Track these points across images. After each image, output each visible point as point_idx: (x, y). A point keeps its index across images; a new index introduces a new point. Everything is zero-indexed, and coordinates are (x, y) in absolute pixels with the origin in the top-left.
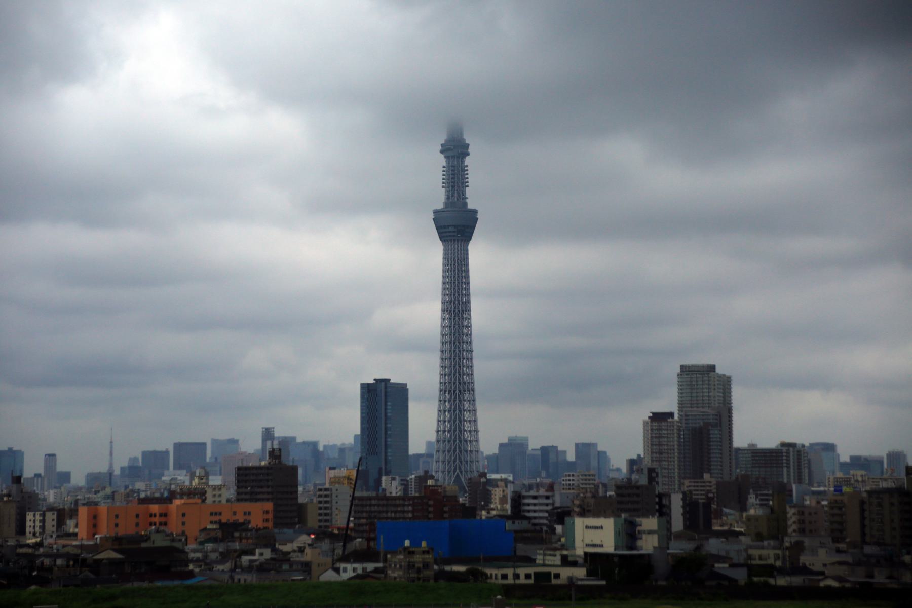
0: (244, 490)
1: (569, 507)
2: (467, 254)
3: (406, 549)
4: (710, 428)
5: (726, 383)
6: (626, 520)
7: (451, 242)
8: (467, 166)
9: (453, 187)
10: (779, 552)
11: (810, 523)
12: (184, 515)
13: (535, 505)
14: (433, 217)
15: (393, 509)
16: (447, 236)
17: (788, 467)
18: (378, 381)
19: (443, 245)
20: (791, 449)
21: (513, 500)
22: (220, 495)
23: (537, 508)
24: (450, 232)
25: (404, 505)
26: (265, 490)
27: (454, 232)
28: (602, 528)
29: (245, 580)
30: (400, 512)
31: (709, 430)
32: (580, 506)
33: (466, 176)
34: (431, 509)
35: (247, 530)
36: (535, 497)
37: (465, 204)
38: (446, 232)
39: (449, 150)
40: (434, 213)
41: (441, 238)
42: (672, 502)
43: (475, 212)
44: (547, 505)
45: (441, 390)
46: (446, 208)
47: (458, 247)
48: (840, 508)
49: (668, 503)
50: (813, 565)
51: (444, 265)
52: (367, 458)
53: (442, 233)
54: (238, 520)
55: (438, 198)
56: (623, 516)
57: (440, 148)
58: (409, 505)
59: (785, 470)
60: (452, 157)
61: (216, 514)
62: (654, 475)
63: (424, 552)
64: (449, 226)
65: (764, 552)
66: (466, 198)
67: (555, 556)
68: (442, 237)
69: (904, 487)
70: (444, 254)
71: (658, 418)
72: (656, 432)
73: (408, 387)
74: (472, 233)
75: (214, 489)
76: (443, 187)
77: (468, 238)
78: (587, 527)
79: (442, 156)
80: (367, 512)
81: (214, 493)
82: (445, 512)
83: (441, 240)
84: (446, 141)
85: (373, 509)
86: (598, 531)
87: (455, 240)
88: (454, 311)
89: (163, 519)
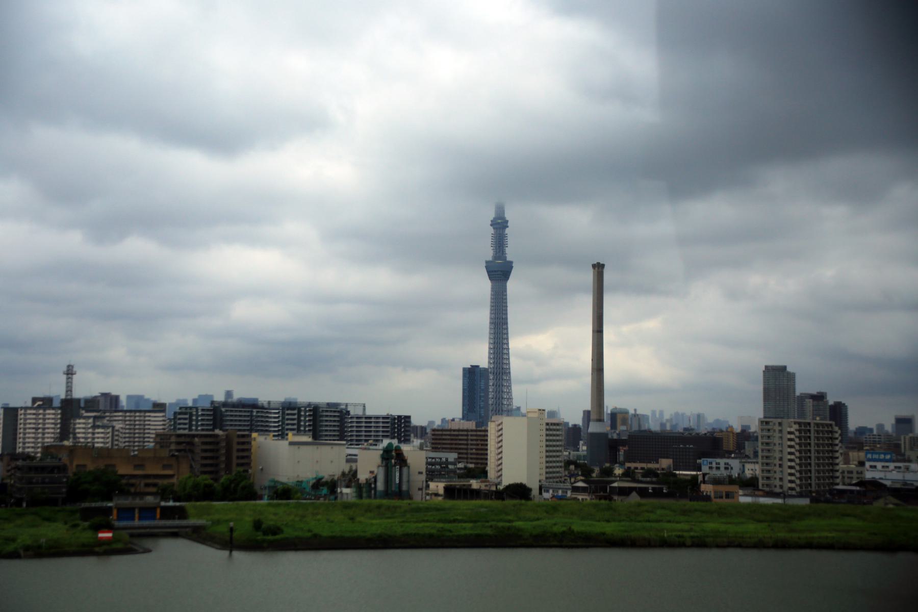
8: (507, 234)
9: (499, 247)
19: (491, 283)
24: (498, 275)
27: (500, 275)
37: (506, 257)
43: (511, 262)
52: (467, 414)
55: (488, 253)
57: (490, 223)
60: (500, 228)
64: (498, 271)
68: (490, 278)
74: (509, 276)
79: (492, 228)
84: (494, 218)
88: (500, 324)
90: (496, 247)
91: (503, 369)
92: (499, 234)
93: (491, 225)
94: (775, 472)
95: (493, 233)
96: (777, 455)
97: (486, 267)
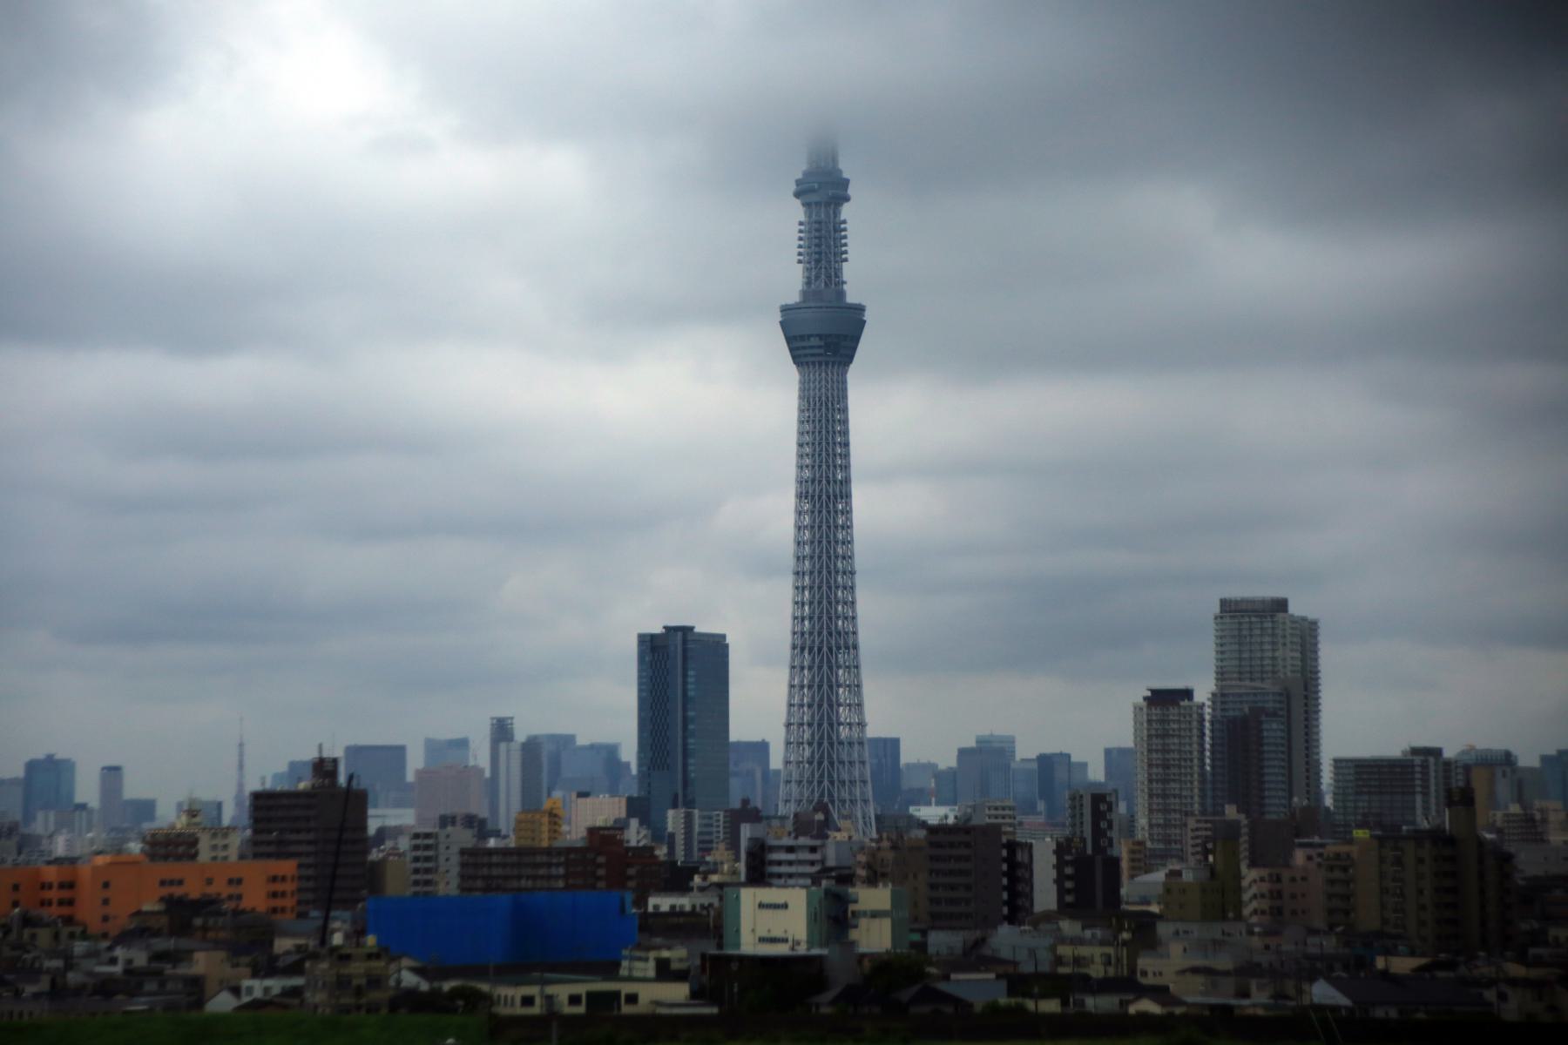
0: (264, 837)
1: (849, 868)
2: (845, 390)
3: (334, 949)
4: (1263, 718)
5: (1307, 634)
6: (827, 892)
7: (814, 367)
8: (844, 222)
9: (818, 261)
10: (1110, 950)
11: (1293, 896)
12: (106, 885)
13: (790, 863)
15: (529, 871)
16: (806, 355)
17: (1426, 794)
19: (800, 373)
20: (1432, 760)
21: (750, 854)
22: (225, 847)
23: (792, 869)
24: (812, 347)
25: (550, 865)
26: (302, 836)
27: (820, 347)
28: (785, 906)
29: (31, 1014)
30: (542, 877)
31: (1261, 723)
32: (869, 866)
33: (843, 241)
34: (601, 872)
35: (219, 914)
36: (790, 849)
37: (841, 294)
38: (804, 348)
39: (812, 191)
40: (781, 311)
42: (1035, 858)
43: (860, 309)
44: (812, 863)
45: (794, 647)
46: (804, 302)
47: (827, 375)
48: (1345, 869)
49: (1026, 860)
50: (1161, 974)
51: (801, 411)
53: (798, 348)
54: (187, 895)
55: (790, 282)
56: (824, 883)
57: (793, 187)
58: (558, 865)
59: (1419, 798)
60: (817, 204)
61: (172, 883)
62: (1103, 807)
63: (370, 956)
64: (809, 336)
65: (1084, 951)
66: (844, 283)
67: (646, 960)
68: (798, 357)
69: (1444, 831)
70: (800, 389)
71: (1164, 700)
72: (1158, 726)
73: (728, 640)
74: (854, 349)
75: (214, 835)
76: (800, 262)
77: (849, 358)
78: (761, 906)
79: (798, 203)
80: (484, 878)
81: (214, 842)
82: (630, 878)
83: (795, 363)
84: (806, 174)
85: (496, 872)
86: (781, 912)
88: (820, 497)
89: (65, 894)
97: (781, 323)
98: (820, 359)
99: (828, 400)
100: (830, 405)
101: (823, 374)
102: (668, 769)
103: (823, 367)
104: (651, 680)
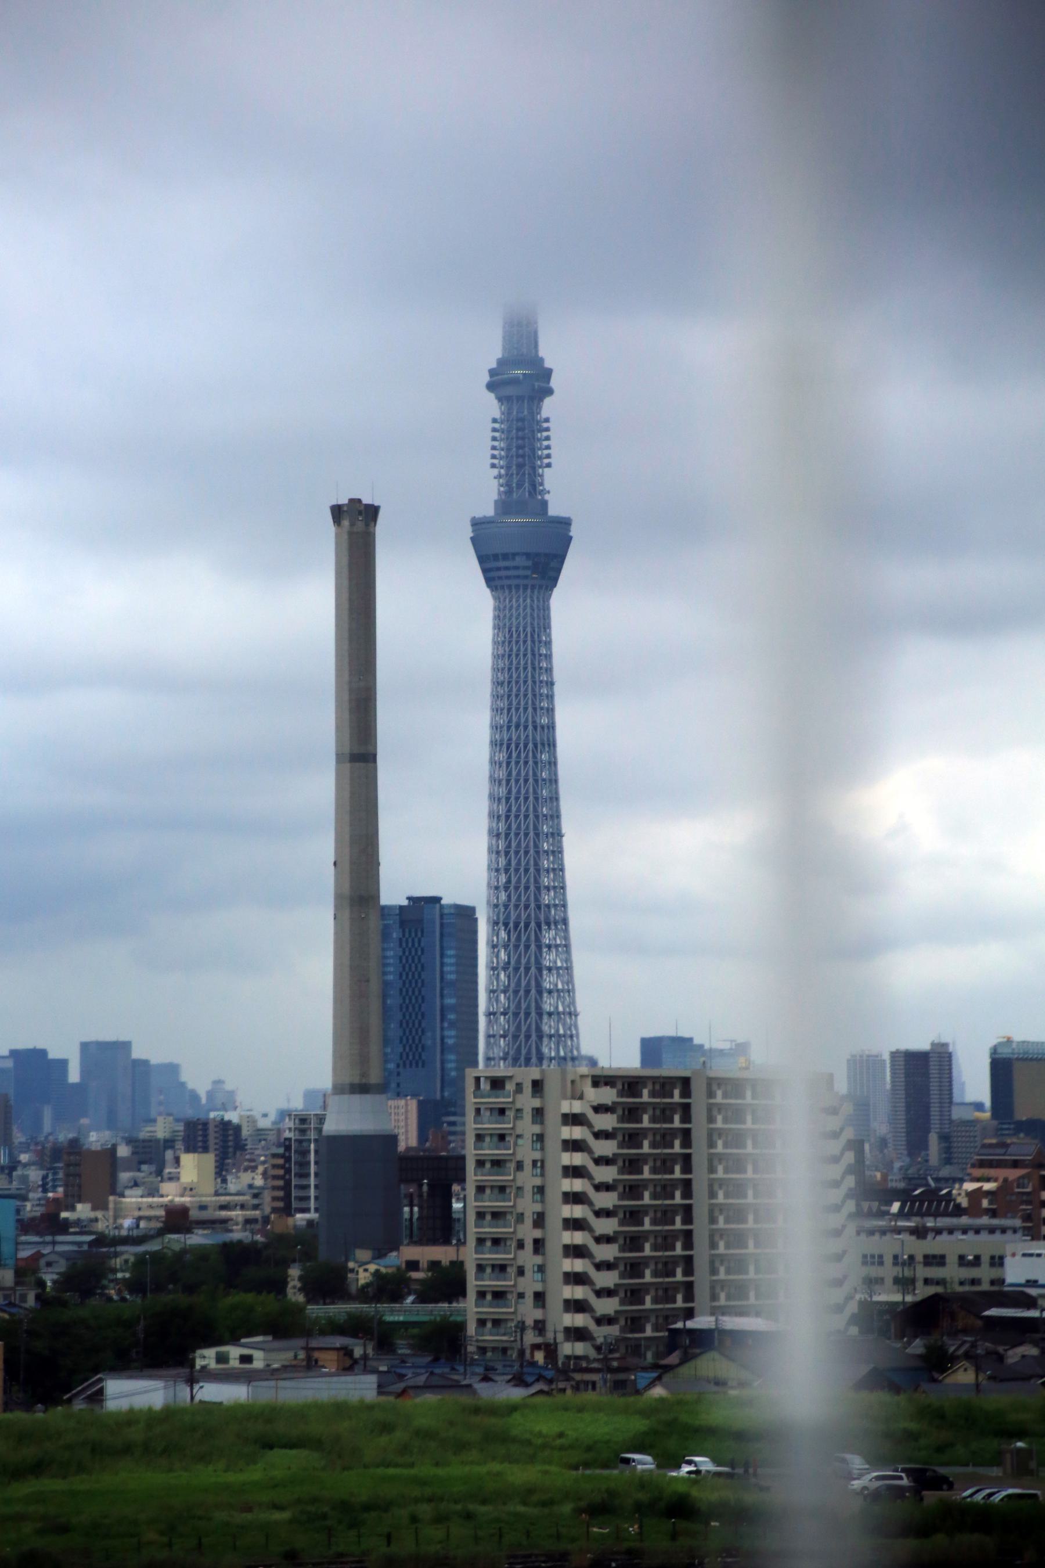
7: (510, 592)
9: (520, 466)
14: (472, 535)
16: (508, 577)
18: (416, 902)
24: (516, 568)
27: (526, 568)
37: (545, 504)
40: (472, 525)
41: (490, 581)
43: (565, 523)
52: (398, 1074)
57: (487, 378)
60: (520, 399)
64: (514, 555)
68: (491, 581)
74: (559, 570)
79: (491, 397)
84: (501, 362)
87: (525, 587)
90: (508, 468)
91: (539, 907)
92: (519, 420)
93: (490, 387)
94: (521, 1272)
95: (497, 415)
96: (528, 1206)
97: (474, 540)
98: (525, 582)
99: (534, 631)
100: (536, 636)
101: (528, 601)
102: (423, 1066)
103: (529, 591)
104: (401, 961)
